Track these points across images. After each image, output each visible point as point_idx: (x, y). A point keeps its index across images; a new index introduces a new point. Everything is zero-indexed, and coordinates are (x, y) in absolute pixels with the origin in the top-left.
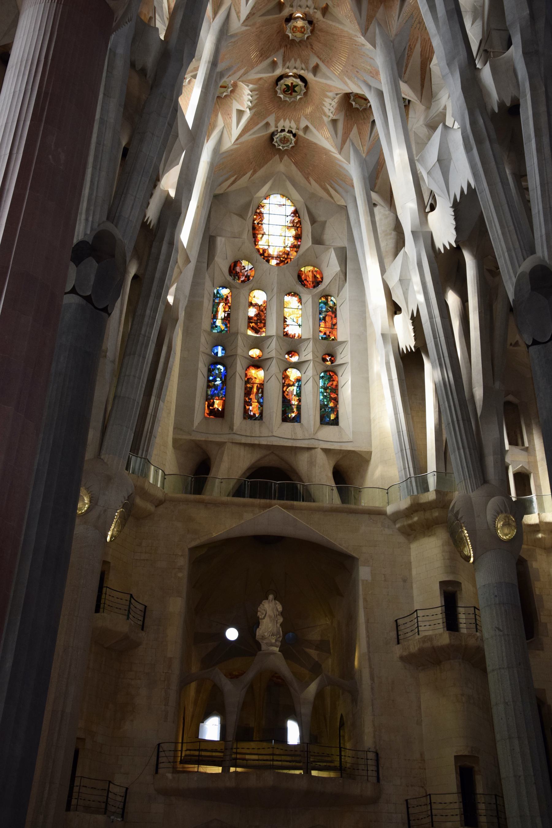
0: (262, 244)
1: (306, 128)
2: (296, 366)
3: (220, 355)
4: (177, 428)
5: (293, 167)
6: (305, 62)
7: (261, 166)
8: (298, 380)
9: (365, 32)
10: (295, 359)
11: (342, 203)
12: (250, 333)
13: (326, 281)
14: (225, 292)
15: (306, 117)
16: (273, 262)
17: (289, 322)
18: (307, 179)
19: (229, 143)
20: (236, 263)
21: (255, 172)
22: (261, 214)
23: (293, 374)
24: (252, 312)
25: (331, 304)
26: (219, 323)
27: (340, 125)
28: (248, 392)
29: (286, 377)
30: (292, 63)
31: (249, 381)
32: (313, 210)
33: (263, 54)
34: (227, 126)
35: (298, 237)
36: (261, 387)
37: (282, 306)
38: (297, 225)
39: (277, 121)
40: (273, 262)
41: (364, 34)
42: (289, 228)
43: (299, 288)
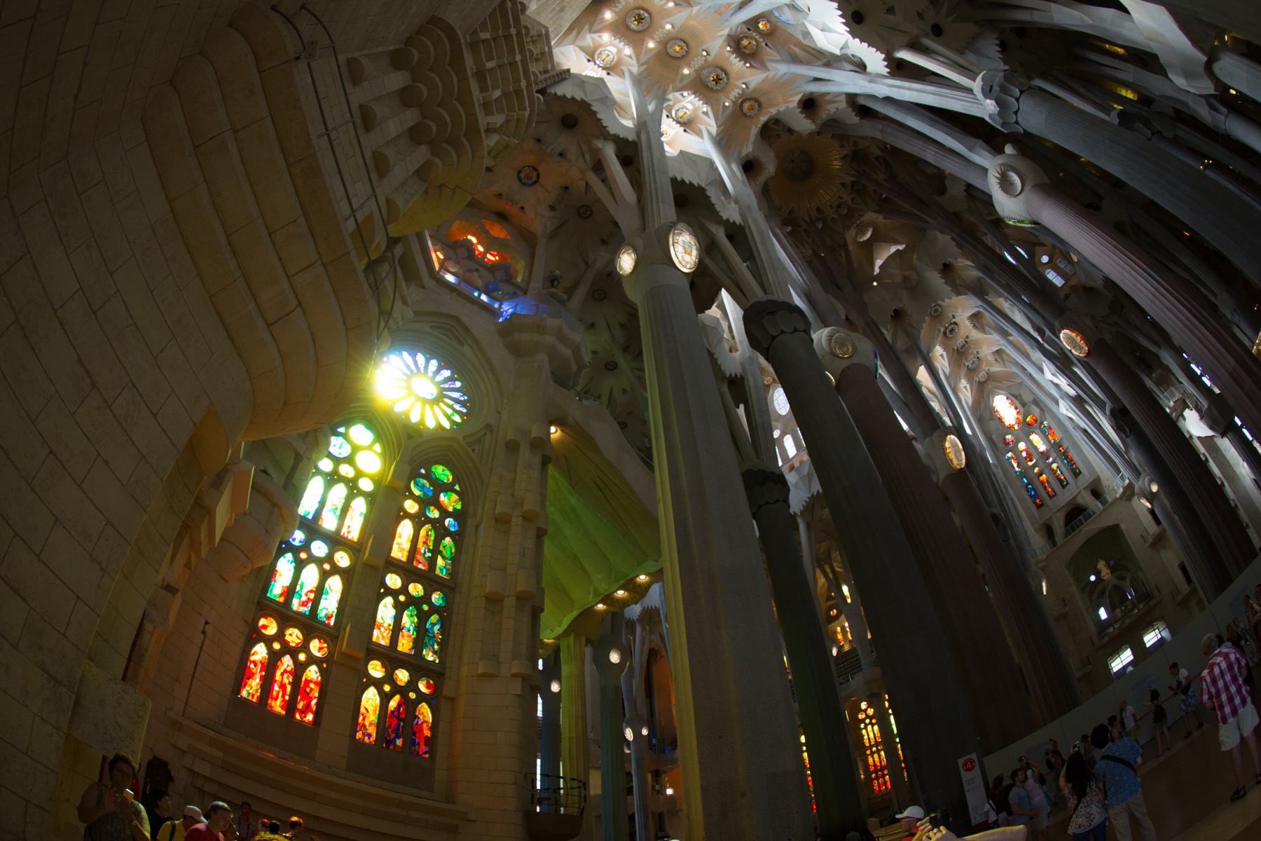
0: (1007, 423)
1: (989, 370)
2: (1053, 462)
3: (1026, 481)
4: (1033, 525)
5: (994, 383)
6: (972, 354)
7: (983, 394)
8: (1058, 467)
9: (985, 332)
10: (1051, 460)
11: (1019, 381)
12: (1030, 464)
13: (1039, 418)
14: (1010, 454)
15: (986, 366)
16: (1016, 427)
17: (1038, 447)
18: (1001, 383)
19: (970, 402)
20: (1005, 439)
21: (983, 397)
22: (997, 411)
23: (1054, 466)
24: (1024, 454)
25: (1046, 425)
26: (1017, 469)
27: (998, 359)
28: (1045, 488)
29: (1053, 470)
30: (969, 358)
31: (1042, 483)
32: (1012, 393)
33: (959, 366)
34: (965, 395)
35: (1016, 408)
36: (1048, 482)
37: (1031, 442)
38: (1012, 403)
39: (978, 376)
40: (1016, 427)
41: (986, 334)
42: (1010, 407)
43: (1032, 430)
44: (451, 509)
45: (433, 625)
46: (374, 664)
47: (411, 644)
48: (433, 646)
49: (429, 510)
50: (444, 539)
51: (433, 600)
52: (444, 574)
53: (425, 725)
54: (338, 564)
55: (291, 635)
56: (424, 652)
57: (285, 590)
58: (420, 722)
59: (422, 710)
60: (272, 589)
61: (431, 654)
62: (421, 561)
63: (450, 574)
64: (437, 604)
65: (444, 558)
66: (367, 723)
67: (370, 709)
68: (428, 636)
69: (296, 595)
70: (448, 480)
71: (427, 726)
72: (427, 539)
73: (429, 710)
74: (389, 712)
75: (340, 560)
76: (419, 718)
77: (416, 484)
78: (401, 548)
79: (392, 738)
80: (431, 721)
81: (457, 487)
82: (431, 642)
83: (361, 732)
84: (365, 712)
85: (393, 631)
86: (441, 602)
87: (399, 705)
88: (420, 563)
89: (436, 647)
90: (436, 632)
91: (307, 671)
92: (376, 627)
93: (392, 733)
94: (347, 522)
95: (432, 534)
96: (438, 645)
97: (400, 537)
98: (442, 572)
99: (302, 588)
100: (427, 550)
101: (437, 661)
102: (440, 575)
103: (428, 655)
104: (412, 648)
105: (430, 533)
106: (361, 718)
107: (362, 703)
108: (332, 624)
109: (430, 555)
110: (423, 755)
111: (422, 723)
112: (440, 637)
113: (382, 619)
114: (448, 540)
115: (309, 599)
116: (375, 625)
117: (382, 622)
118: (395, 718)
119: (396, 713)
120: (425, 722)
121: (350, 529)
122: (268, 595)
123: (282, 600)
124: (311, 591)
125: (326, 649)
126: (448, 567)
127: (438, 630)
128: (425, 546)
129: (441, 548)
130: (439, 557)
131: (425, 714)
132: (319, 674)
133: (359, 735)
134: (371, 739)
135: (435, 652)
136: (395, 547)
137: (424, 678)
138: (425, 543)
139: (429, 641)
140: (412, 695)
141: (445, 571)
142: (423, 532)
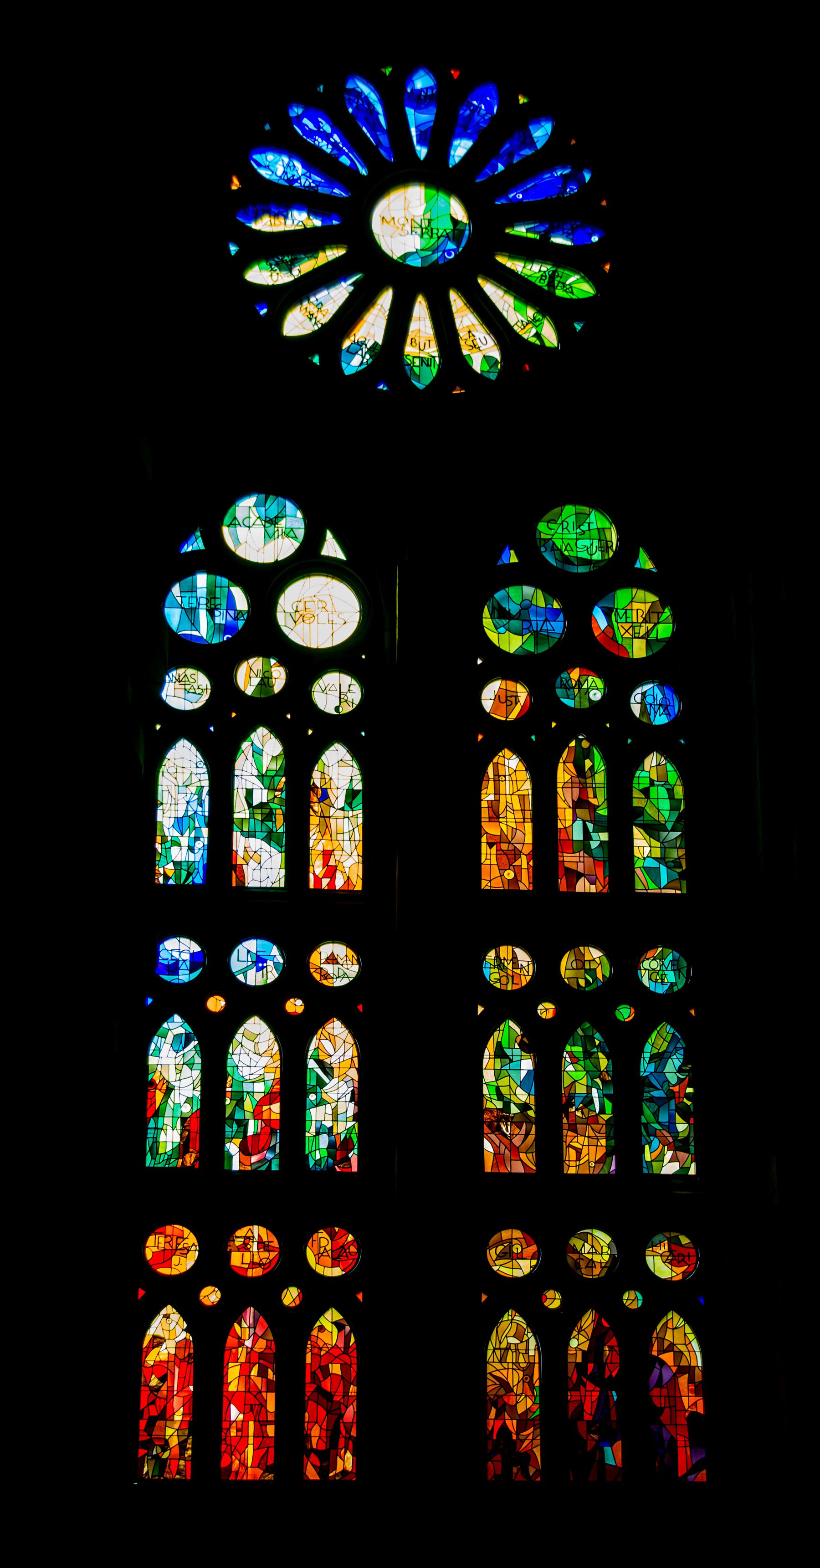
44: (639, 650)
45: (660, 1058)
46: (501, 1242)
47: (603, 1142)
48: (672, 1123)
49: (567, 687)
50: (639, 763)
51: (645, 981)
52: (664, 881)
53: (683, 1380)
54: (325, 982)
55: (244, 1248)
56: (648, 1157)
57: (196, 1126)
58: (666, 1376)
59: (669, 1336)
60: (156, 1141)
61: (669, 1154)
62: (580, 868)
63: (682, 876)
64: (660, 990)
65: (653, 829)
66: (512, 1425)
67: (514, 1378)
68: (652, 1099)
69: (230, 1130)
70: (605, 547)
71: (691, 1380)
72: (583, 789)
73: (688, 1330)
74: (571, 1368)
75: (329, 968)
76: (663, 1363)
77: (501, 613)
78: (505, 853)
79: (590, 1445)
80: (700, 1364)
81: (644, 562)
82: (664, 1118)
83: (498, 1457)
84: (502, 1392)
85: (539, 1121)
86: (671, 977)
87: (597, 1340)
88: (579, 875)
89: (682, 1126)
90: (673, 1078)
91: (315, 1332)
92: (486, 1130)
93: (589, 1431)
94: (317, 843)
95: (597, 763)
96: (685, 1118)
97: (495, 817)
98: (656, 879)
99: (240, 1103)
100: (590, 826)
101: (692, 1171)
102: (653, 888)
103: (660, 1158)
104: (607, 1155)
105: (588, 763)
106: (493, 1412)
107: (490, 1369)
108: (355, 1169)
109: (604, 836)
110: (691, 1478)
111: (675, 1377)
112: (690, 1090)
113: (500, 1096)
114: (652, 761)
115: (268, 1122)
116: (481, 1121)
117: (499, 1105)
118: (590, 1386)
119: (591, 1367)
120: (682, 1370)
121: (332, 863)
122: (149, 1161)
123: (190, 1159)
124: (269, 1098)
125: (353, 1249)
126: (674, 854)
127: (680, 1070)
128: (582, 813)
129: (638, 801)
130: (638, 833)
131: (682, 1348)
132: (348, 1328)
133: (493, 1468)
134: (532, 1471)
135: (679, 1145)
136: (488, 855)
137: (656, 1239)
138: (580, 803)
139: (656, 1115)
140: (632, 1299)
141: (663, 869)
142: (564, 774)
